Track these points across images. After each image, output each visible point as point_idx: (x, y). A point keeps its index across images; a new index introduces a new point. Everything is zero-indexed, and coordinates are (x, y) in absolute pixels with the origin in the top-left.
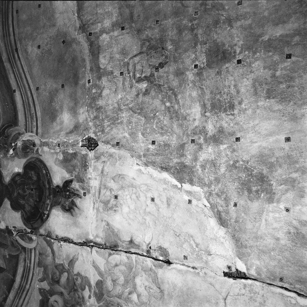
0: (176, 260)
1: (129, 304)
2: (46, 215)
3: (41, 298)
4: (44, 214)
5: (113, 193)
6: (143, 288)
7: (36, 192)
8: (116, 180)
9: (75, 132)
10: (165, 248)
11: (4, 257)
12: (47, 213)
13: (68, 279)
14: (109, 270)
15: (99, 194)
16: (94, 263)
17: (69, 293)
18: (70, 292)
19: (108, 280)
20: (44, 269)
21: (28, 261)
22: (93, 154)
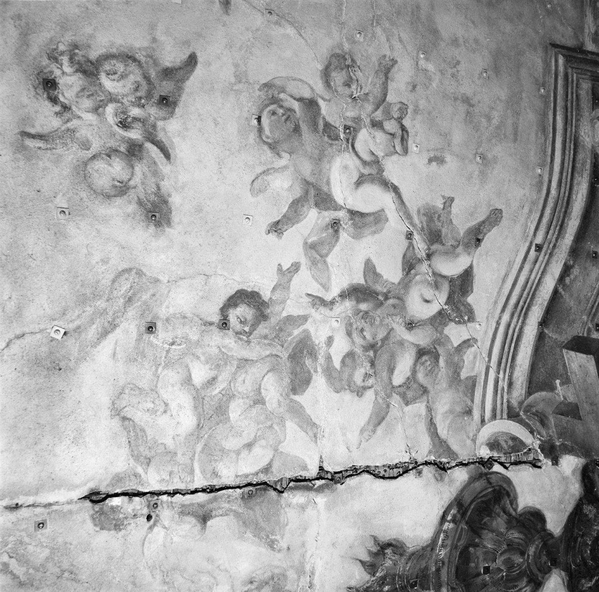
0: (70, 512)
1: (217, 351)
2: (449, 518)
3: (470, 299)
4: (454, 521)
6: (173, 406)
7: (477, 567)
10: (104, 531)
11: (566, 381)
12: (446, 526)
13: (391, 370)
14: (271, 427)
16: (315, 436)
17: (389, 333)
18: (386, 339)
19: (275, 401)
20: (459, 375)
21: (503, 384)
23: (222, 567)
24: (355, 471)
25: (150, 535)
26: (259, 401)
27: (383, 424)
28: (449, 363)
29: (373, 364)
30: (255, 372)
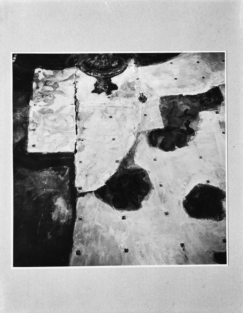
0: (78, 156)
1: (41, 131)
2: (90, 74)
4: (91, 73)
5: (113, 115)
6: (54, 139)
7: (104, 66)
8: (122, 116)
9: (148, 89)
13: (49, 91)
15: (111, 107)
17: (39, 93)
18: (41, 93)
22: (137, 101)
23: (97, 124)
24: (75, 97)
25: (87, 140)
26: (55, 120)
27: (63, 92)
28: (49, 78)
29: (47, 95)
30: (47, 121)
